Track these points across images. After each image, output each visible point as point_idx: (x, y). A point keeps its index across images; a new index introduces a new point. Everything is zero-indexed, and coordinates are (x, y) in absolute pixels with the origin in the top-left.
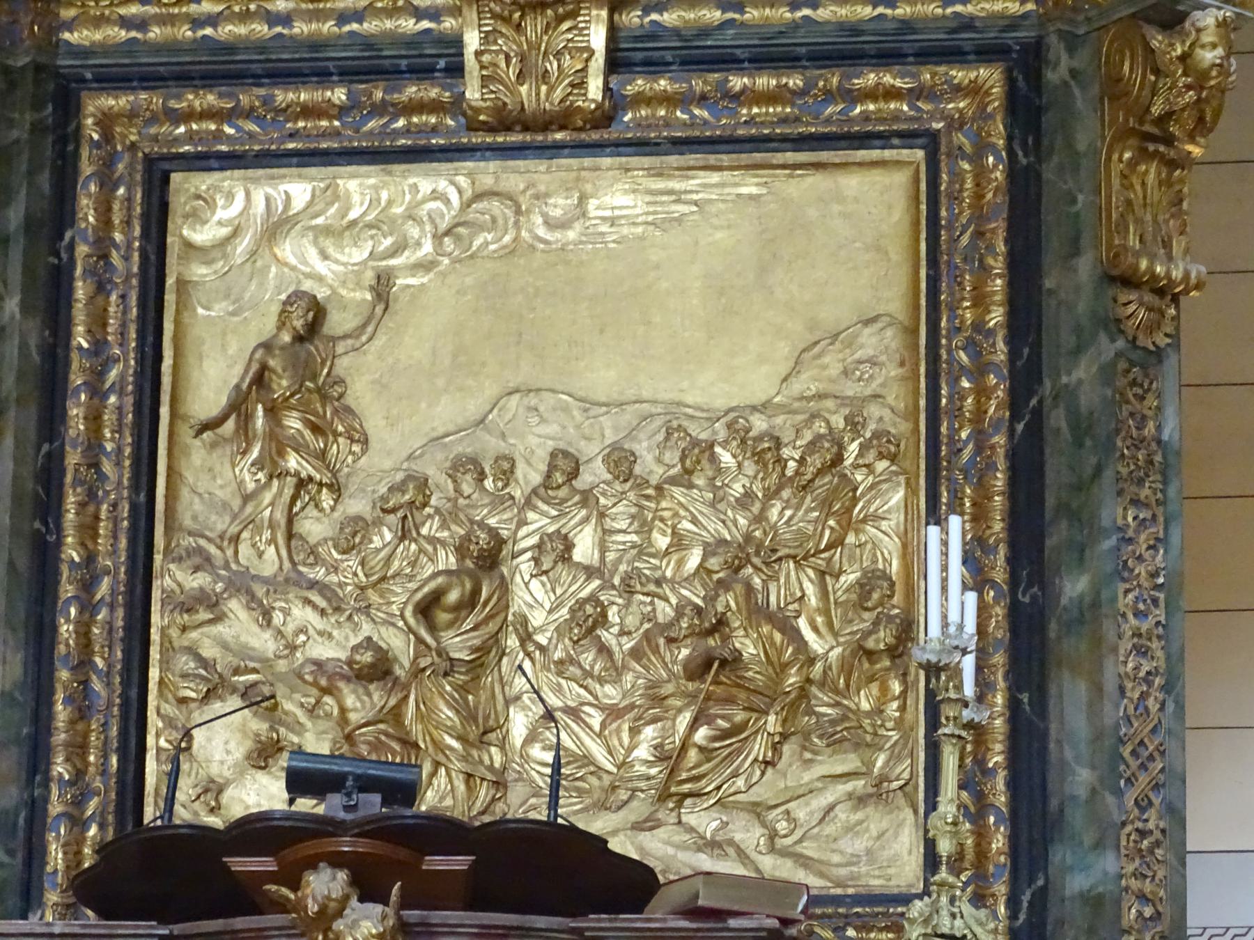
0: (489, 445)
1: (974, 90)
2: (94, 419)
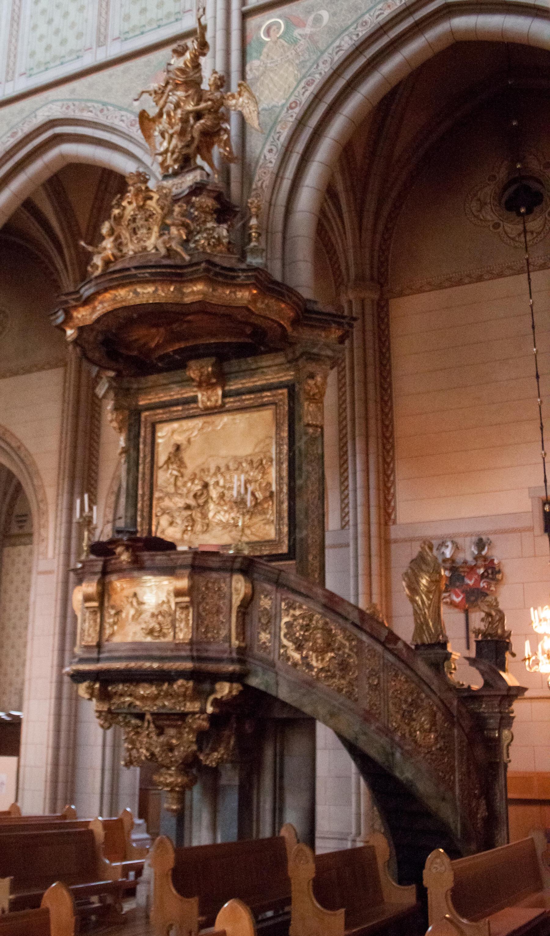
0: (205, 466)
1: (282, 394)
2: (144, 469)
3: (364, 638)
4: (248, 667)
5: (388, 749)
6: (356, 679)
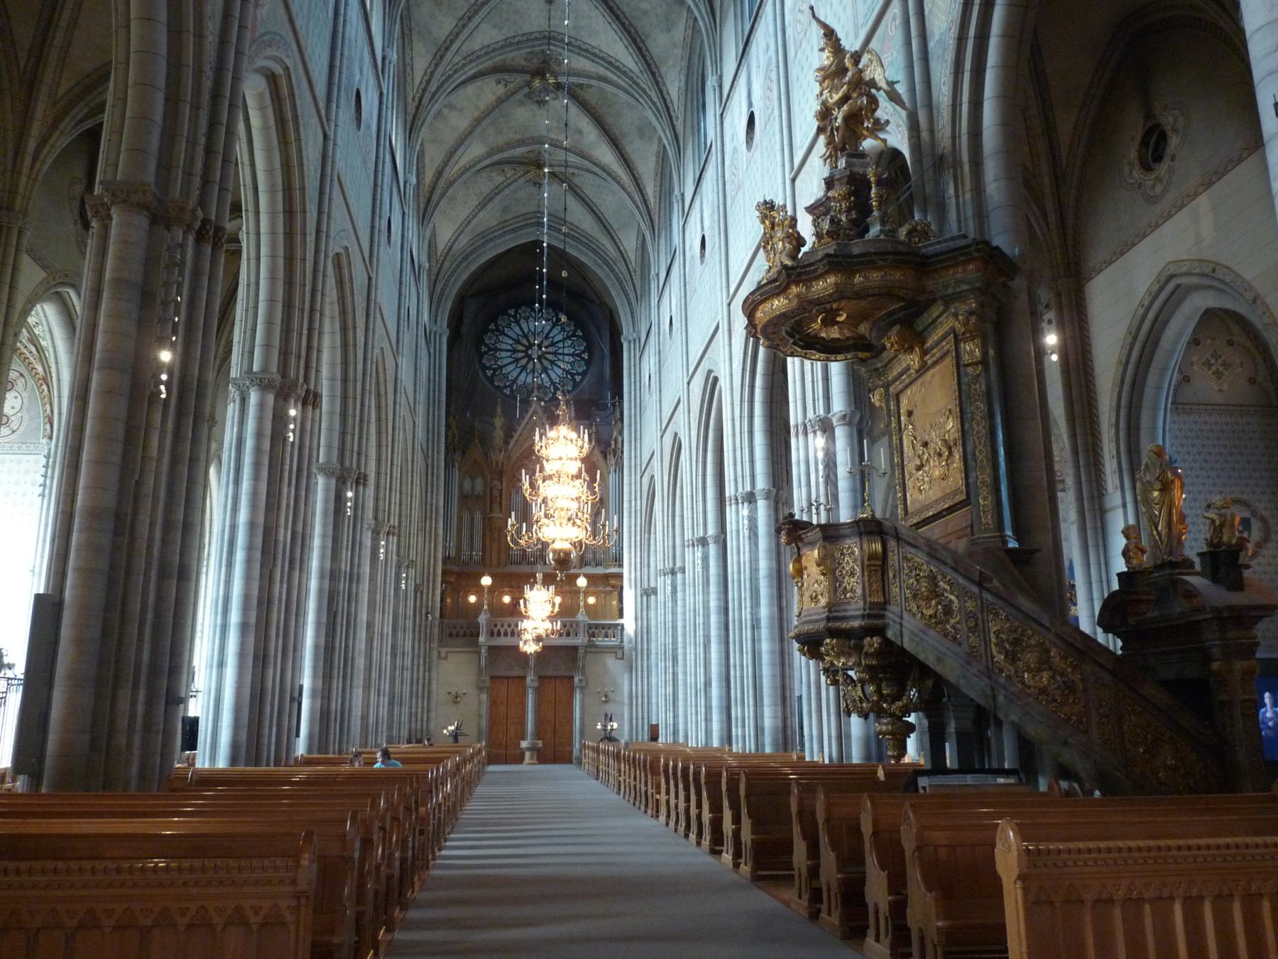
3: (961, 580)
4: (886, 620)
5: (989, 692)
6: (958, 623)
